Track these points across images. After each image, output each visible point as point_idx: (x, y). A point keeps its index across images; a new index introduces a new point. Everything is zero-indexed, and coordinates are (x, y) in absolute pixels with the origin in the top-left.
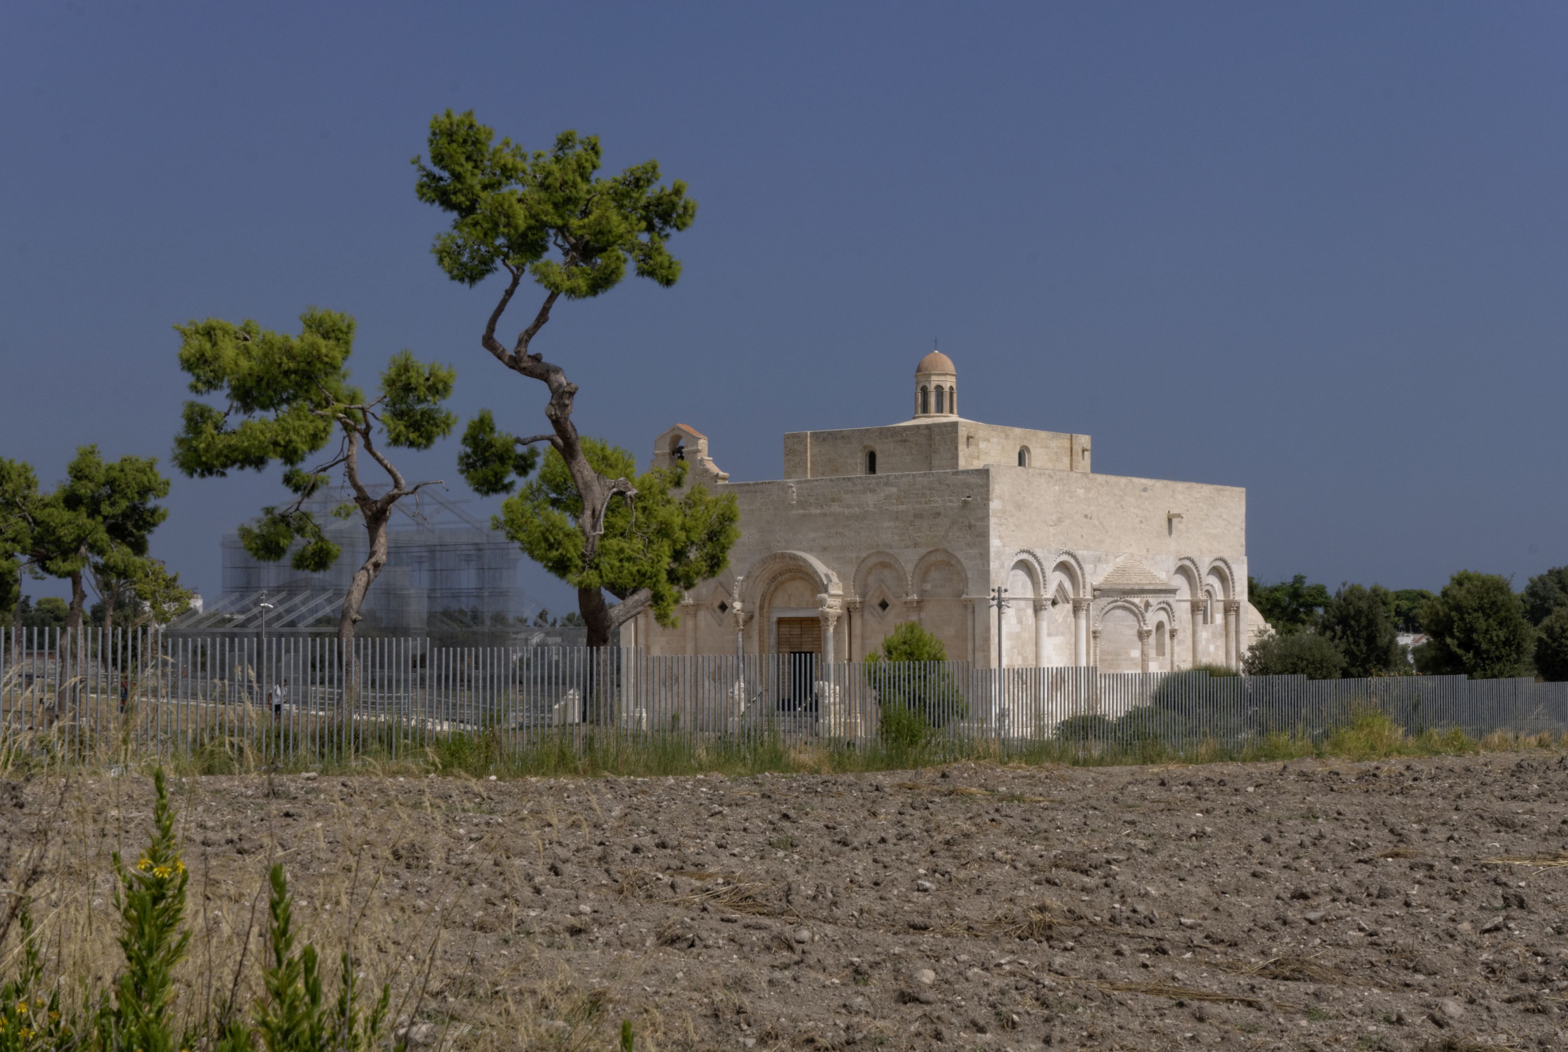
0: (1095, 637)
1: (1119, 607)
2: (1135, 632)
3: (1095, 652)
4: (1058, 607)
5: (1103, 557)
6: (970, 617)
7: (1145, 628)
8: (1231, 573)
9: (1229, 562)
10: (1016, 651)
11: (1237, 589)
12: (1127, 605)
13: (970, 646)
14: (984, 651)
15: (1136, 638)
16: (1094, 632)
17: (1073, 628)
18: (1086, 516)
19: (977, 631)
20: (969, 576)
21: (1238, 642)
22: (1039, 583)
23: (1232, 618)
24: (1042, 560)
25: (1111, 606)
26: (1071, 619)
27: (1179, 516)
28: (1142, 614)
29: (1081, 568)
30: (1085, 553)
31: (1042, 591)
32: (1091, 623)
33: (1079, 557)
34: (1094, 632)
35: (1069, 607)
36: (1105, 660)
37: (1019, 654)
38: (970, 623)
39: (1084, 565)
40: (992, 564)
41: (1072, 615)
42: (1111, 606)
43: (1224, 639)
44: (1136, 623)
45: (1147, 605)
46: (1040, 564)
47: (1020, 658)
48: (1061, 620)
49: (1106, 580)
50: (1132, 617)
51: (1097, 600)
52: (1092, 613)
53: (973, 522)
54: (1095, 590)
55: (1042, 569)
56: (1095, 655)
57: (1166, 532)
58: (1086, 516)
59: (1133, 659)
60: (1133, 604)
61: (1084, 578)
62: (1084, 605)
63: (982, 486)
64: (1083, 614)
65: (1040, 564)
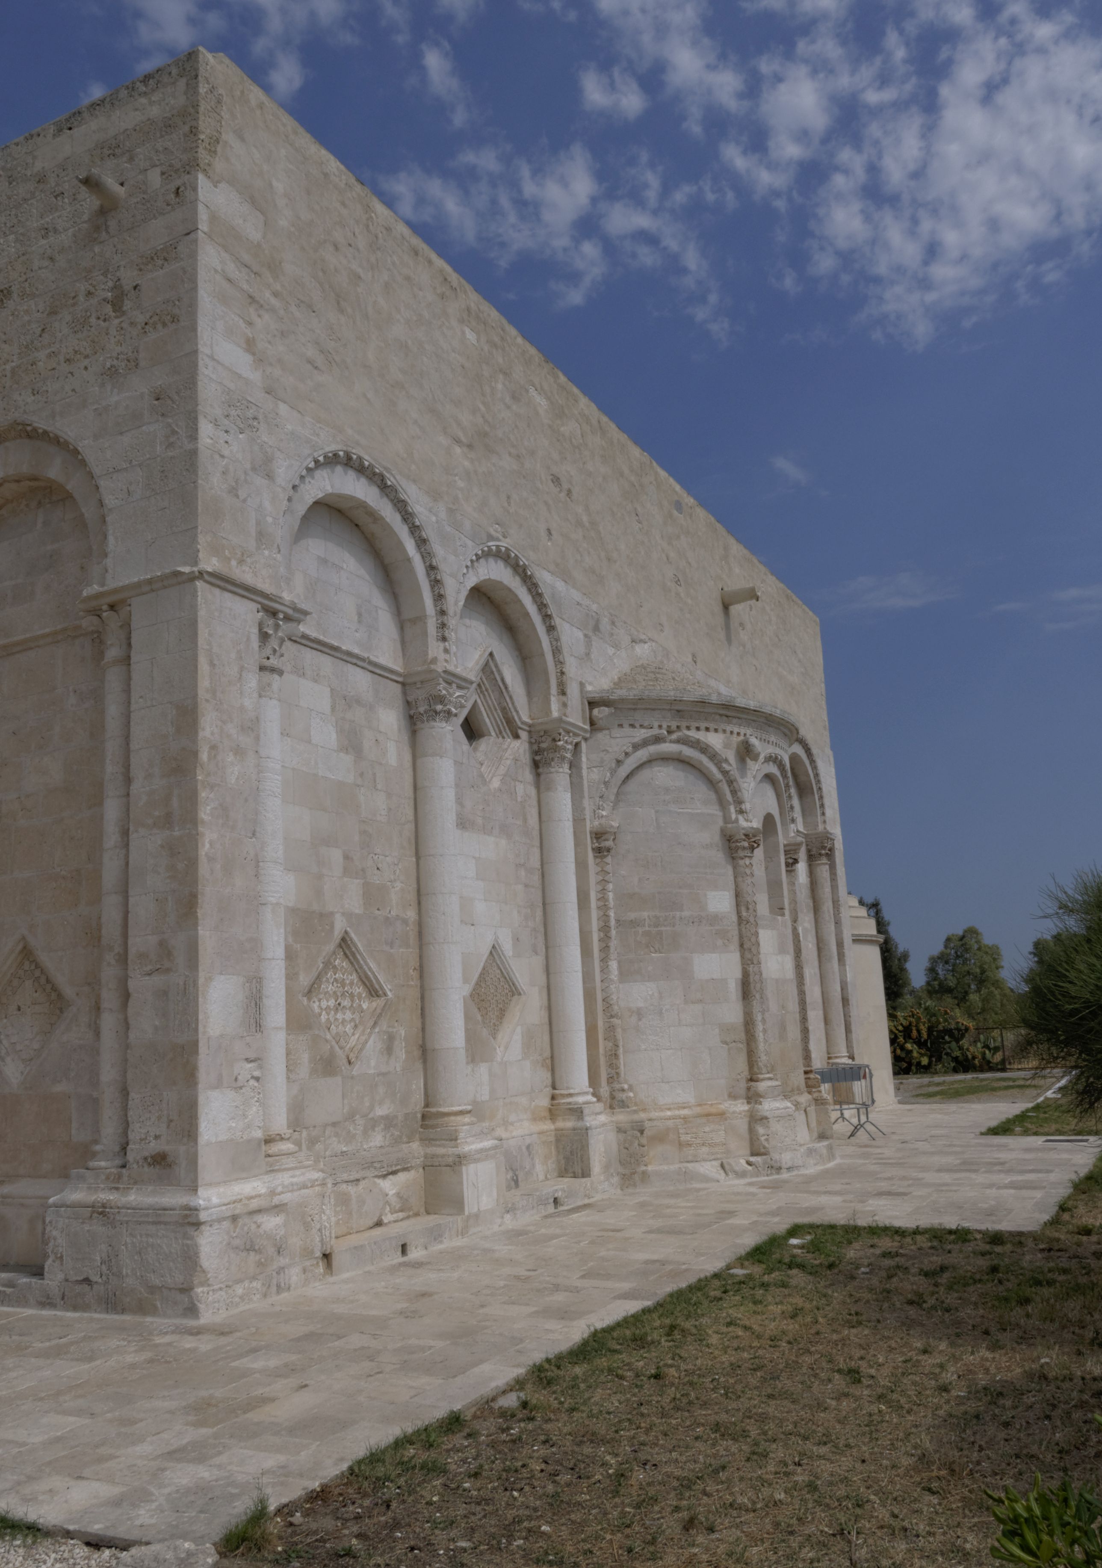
0: (600, 852)
1: (665, 759)
2: (711, 836)
3: (603, 899)
4: (483, 745)
5: (605, 622)
6: (113, 679)
7: (743, 823)
8: (817, 775)
9: (815, 751)
10: (336, 855)
11: (829, 812)
12: (688, 752)
13: (112, 810)
14: (167, 821)
15: (718, 856)
16: (598, 835)
17: (533, 820)
18: (556, 480)
19: (139, 733)
20: (110, 500)
21: (838, 923)
22: (420, 619)
23: (823, 871)
24: (429, 533)
25: (642, 754)
26: (525, 788)
27: (752, 595)
28: (730, 782)
29: (551, 628)
30: (560, 585)
31: (435, 649)
32: (586, 803)
33: (543, 589)
34: (598, 835)
35: (519, 748)
36: (634, 923)
37: (346, 871)
38: (113, 710)
39: (557, 621)
40: (206, 430)
41: (528, 775)
42: (642, 754)
43: (811, 915)
44: (714, 810)
45: (746, 752)
46: (422, 542)
47: (354, 886)
48: (496, 783)
49: (618, 684)
50: (702, 791)
51: (599, 736)
52: (590, 775)
53: (128, 277)
54: (592, 704)
55: (431, 568)
56: (604, 908)
57: (722, 635)
58: (556, 480)
59: (715, 919)
60: (704, 749)
61: (559, 663)
62: (565, 743)
63: (168, 126)
64: (560, 775)
65: (422, 542)
